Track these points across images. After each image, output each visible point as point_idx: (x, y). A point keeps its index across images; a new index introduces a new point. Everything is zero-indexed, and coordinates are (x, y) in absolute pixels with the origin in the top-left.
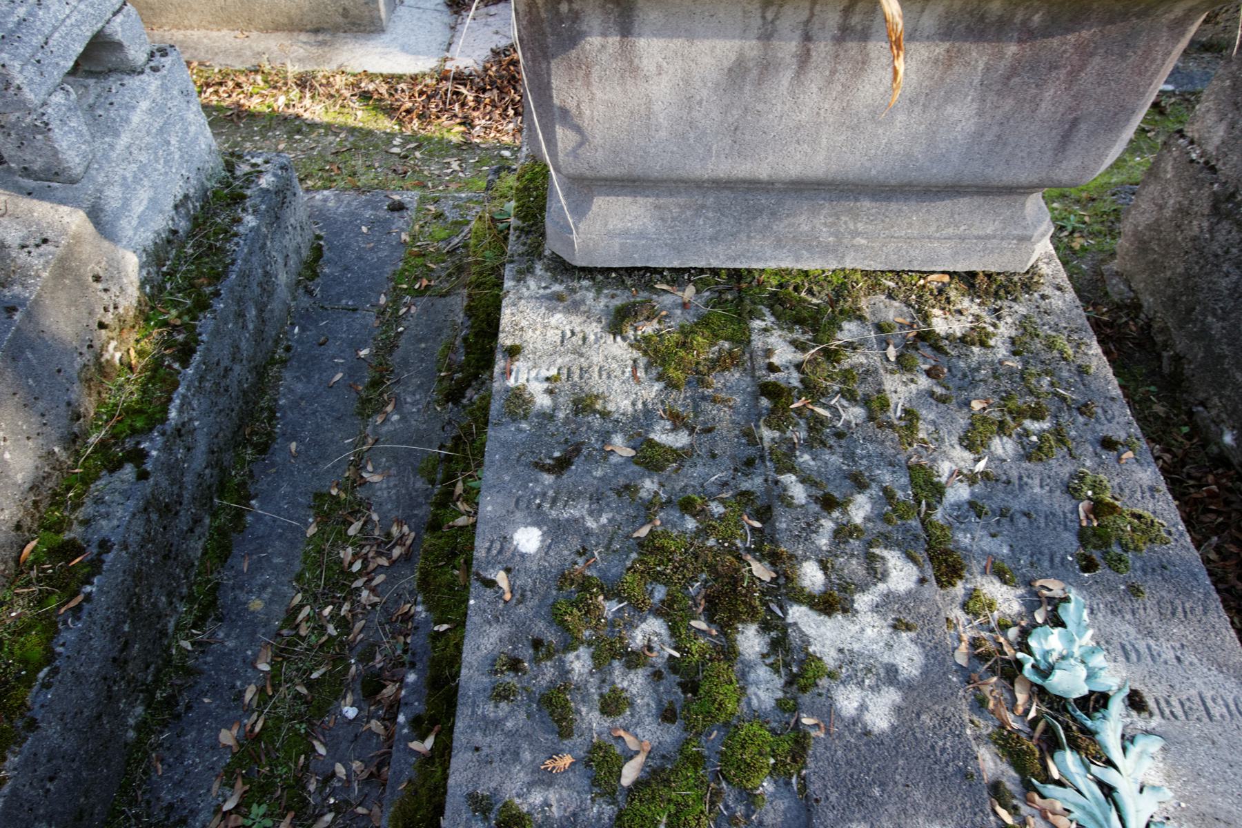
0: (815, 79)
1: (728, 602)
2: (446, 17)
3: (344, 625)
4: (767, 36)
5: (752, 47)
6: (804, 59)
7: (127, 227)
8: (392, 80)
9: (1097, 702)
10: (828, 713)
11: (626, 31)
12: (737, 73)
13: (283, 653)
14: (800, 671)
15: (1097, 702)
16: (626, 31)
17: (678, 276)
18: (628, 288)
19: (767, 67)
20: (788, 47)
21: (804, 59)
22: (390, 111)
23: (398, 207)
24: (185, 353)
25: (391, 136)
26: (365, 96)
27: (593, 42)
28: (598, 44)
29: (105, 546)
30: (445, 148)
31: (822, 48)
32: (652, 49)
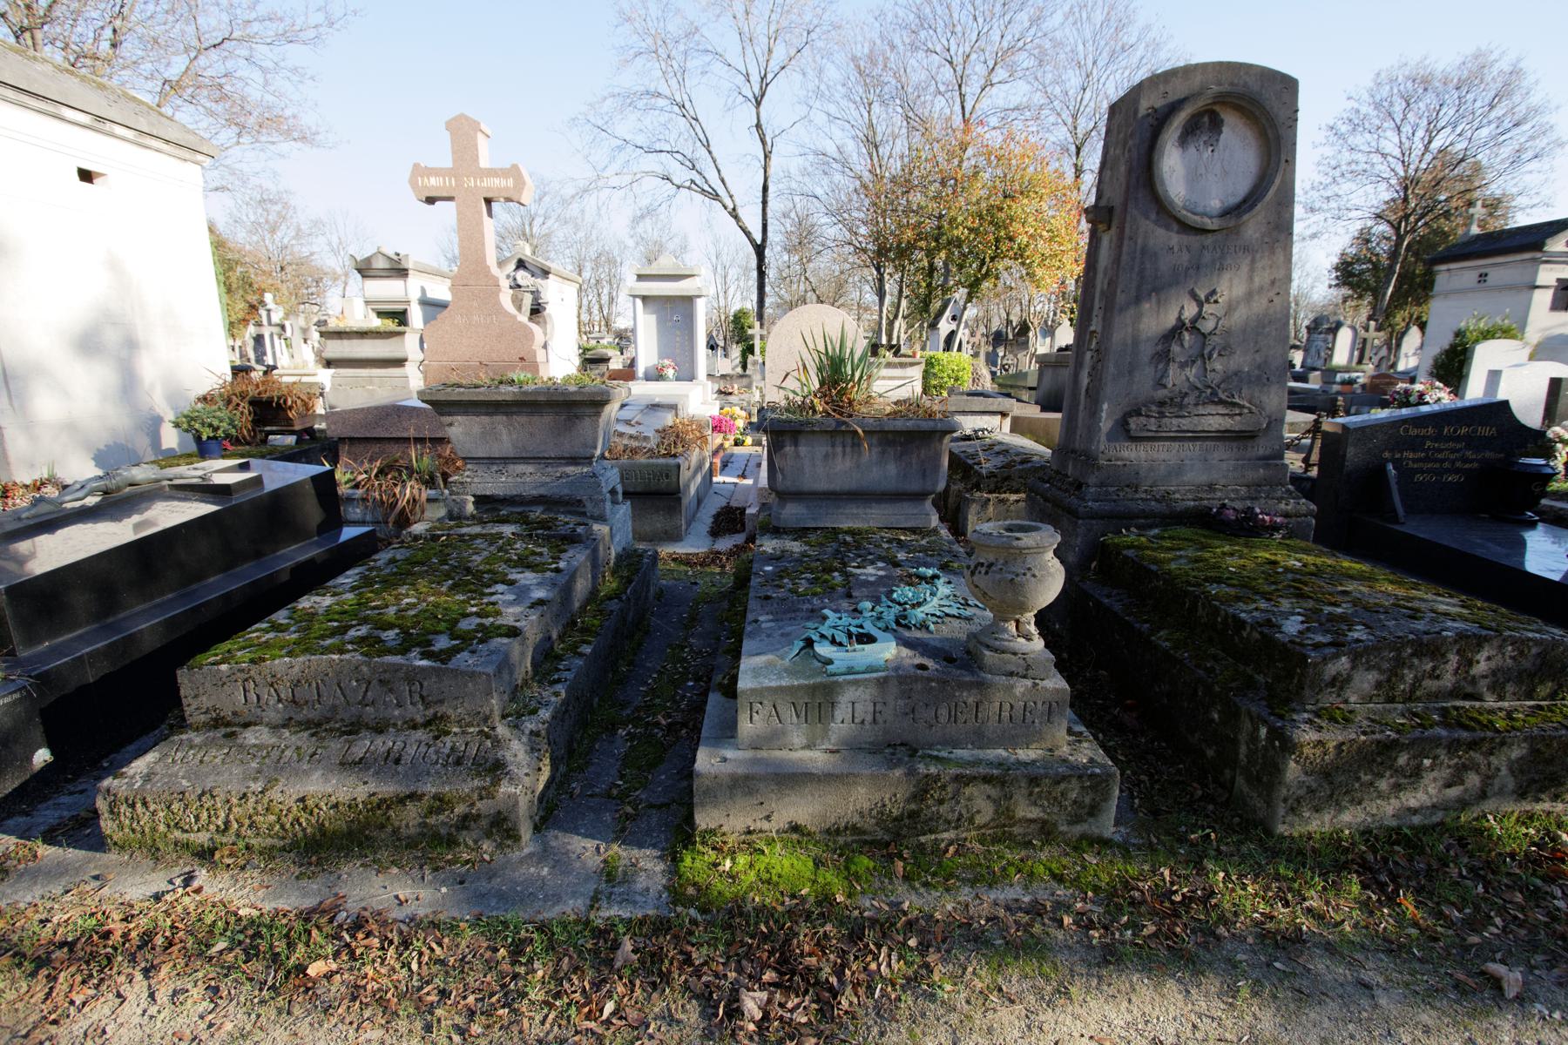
4: (833, 446)
5: (830, 449)
7: (617, 539)
9: (937, 577)
11: (796, 445)
12: (826, 456)
13: (660, 673)
14: (847, 575)
16: (796, 445)
17: (816, 529)
19: (834, 455)
20: (839, 449)
24: (630, 581)
26: (674, 560)
27: (787, 449)
28: (789, 449)
32: (803, 450)
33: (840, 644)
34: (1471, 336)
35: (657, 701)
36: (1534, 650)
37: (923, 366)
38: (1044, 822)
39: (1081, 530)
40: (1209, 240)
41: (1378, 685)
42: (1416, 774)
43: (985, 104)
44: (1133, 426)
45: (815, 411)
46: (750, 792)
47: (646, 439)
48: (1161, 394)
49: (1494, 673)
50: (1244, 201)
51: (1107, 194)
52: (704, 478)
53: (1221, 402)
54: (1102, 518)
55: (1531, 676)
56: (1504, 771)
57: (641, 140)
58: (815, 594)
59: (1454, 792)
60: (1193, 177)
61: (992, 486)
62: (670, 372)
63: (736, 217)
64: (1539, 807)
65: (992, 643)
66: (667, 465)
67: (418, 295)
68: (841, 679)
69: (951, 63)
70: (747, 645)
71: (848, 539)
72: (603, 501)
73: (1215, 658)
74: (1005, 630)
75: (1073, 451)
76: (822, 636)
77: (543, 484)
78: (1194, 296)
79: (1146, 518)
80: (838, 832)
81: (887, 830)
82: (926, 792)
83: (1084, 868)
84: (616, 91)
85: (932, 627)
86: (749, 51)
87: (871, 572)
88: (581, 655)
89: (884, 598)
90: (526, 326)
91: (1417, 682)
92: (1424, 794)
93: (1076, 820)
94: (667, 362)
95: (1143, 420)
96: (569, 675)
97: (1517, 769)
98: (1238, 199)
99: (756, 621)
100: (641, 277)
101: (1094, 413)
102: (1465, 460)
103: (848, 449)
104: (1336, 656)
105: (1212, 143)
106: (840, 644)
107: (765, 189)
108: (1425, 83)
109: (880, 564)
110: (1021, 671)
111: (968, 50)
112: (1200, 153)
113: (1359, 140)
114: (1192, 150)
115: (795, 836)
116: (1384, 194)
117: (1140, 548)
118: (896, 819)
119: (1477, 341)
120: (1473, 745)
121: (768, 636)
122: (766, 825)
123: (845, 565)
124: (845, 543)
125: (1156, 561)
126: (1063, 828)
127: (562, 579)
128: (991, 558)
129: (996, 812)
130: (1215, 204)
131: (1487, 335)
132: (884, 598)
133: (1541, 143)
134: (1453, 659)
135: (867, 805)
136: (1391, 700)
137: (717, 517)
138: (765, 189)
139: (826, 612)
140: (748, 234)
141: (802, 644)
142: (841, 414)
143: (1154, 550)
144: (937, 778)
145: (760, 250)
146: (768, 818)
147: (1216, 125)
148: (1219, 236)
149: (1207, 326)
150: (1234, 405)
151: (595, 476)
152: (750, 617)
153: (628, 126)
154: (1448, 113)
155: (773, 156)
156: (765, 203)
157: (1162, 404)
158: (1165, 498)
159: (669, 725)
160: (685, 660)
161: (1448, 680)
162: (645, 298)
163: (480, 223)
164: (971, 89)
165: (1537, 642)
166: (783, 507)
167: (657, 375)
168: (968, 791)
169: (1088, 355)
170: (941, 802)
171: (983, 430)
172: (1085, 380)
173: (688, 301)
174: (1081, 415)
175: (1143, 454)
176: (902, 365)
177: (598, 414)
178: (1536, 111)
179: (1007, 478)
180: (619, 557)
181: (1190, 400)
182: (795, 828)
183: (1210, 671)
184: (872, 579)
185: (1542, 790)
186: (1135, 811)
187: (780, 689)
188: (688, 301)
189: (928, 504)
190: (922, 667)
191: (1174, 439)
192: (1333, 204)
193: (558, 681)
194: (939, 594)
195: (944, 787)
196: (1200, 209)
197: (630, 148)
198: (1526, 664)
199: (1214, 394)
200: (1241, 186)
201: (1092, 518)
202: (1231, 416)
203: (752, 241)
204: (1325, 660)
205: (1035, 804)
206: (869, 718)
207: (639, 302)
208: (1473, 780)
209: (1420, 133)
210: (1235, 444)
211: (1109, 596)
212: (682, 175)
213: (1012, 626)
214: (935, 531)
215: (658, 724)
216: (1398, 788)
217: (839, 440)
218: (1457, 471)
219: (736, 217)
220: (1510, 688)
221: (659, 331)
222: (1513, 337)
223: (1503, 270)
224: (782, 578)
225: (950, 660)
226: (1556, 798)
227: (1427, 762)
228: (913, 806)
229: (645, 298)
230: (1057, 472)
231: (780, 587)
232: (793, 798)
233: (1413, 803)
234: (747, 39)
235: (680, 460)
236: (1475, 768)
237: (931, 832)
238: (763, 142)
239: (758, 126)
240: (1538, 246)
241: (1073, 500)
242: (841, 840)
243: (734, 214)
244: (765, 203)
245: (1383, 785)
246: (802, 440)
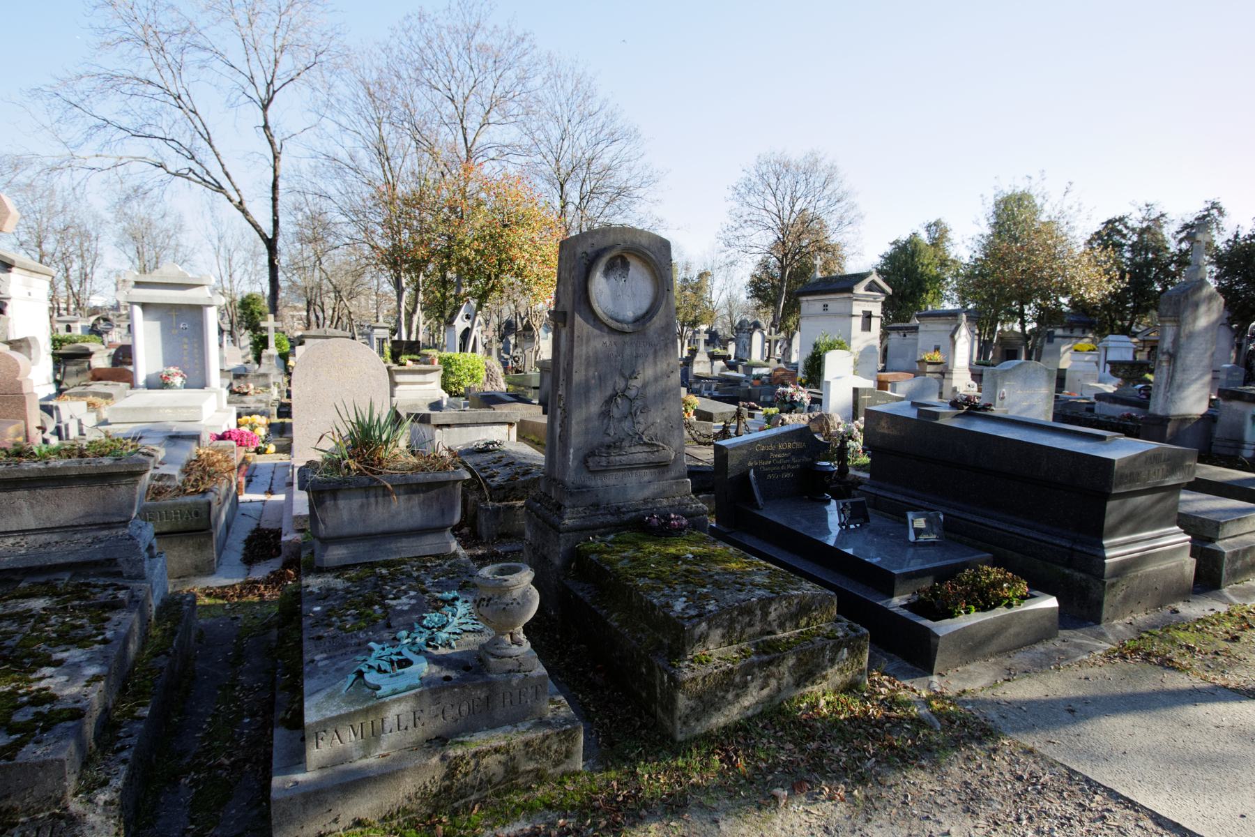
0: (380, 509)
1: (369, 604)
2: (245, 567)
3: (238, 706)
5: (364, 500)
6: (377, 503)
8: (223, 588)
9: (456, 599)
10: (394, 610)
11: (335, 499)
12: (362, 506)
13: (213, 716)
14: (386, 607)
15: (456, 599)
18: (340, 570)
19: (369, 504)
20: (372, 500)
21: (377, 503)
22: (223, 597)
23: (236, 618)
24: (174, 633)
25: (224, 605)
29: (162, 668)
30: (252, 604)
31: (380, 499)
32: (341, 503)
33: (385, 672)
34: (822, 348)
35: (216, 744)
37: (441, 372)
38: (538, 770)
39: (562, 542)
40: (627, 339)
41: (723, 636)
42: (745, 685)
43: (482, 139)
44: (591, 464)
45: (349, 469)
46: (320, 804)
47: (170, 477)
48: (607, 440)
50: (647, 312)
51: (562, 302)
52: (231, 504)
54: (576, 530)
56: (787, 674)
57: (125, 121)
58: (360, 629)
59: (765, 692)
60: (615, 297)
61: (502, 496)
62: (178, 381)
63: (245, 212)
64: (806, 690)
65: (494, 651)
66: (196, 504)
68: (387, 699)
69: (453, 101)
70: (308, 685)
71: (384, 571)
72: (142, 561)
73: (643, 631)
74: (503, 641)
75: (554, 480)
76: (370, 667)
77: (72, 553)
78: (623, 375)
79: (605, 527)
80: (392, 817)
81: (428, 806)
82: (456, 769)
83: (565, 795)
84: (95, 70)
85: (454, 644)
86: (253, 56)
87: (404, 603)
88: (140, 719)
89: (416, 625)
90: (8, 357)
91: (743, 629)
92: (752, 698)
93: (557, 764)
94: (172, 370)
96: (133, 741)
97: (792, 670)
98: (644, 311)
99: (313, 661)
100: (138, 284)
101: (565, 454)
102: (792, 464)
103: (380, 499)
104: (699, 623)
106: (385, 672)
107: (275, 187)
108: (787, 167)
109: (412, 593)
110: (516, 668)
111: (467, 92)
112: (616, 281)
113: (752, 199)
114: (612, 279)
115: (358, 829)
116: (771, 238)
117: (600, 552)
118: (435, 795)
119: (825, 351)
120: (770, 663)
121: (325, 673)
122: (334, 827)
123: (384, 597)
124: (382, 577)
125: (609, 563)
126: (551, 771)
127: (114, 651)
128: (490, 595)
129: (506, 771)
130: (629, 314)
131: (831, 347)
132: (416, 625)
133: (852, 214)
134: (758, 612)
135: (413, 791)
136: (731, 644)
137: (249, 542)
138: (275, 187)
139: (372, 644)
140: (259, 231)
141: (354, 676)
142: (372, 472)
143: (609, 553)
144: (462, 758)
145: (271, 245)
146: (336, 821)
147: (625, 265)
148: (634, 337)
149: (632, 393)
151: (131, 538)
152: (307, 658)
154: (801, 189)
155: (282, 156)
156: (275, 199)
157: (609, 447)
158: (618, 511)
159: (233, 764)
160: (237, 698)
161: (758, 628)
162: (144, 306)
164: (472, 124)
165: (797, 596)
166: (325, 550)
167: (160, 383)
168: (484, 762)
169: (559, 411)
170: (466, 774)
171: (493, 443)
172: (558, 430)
173: (197, 310)
174: (558, 454)
175: (599, 483)
176: (424, 372)
177: (136, 482)
178: (846, 193)
179: (513, 489)
180: (160, 610)
181: (626, 443)
182: (358, 823)
183: (639, 640)
184: (406, 608)
186: (599, 746)
187: (340, 718)
188: (197, 310)
189: (448, 533)
190: (447, 678)
191: (619, 470)
192: (742, 242)
193: (123, 748)
194: (459, 615)
195: (468, 763)
196: (620, 317)
198: (793, 609)
199: (641, 438)
200: (644, 304)
201: (568, 531)
202: (653, 453)
203: (263, 236)
204: (694, 627)
205: (531, 759)
206: (411, 724)
207: (138, 311)
208: (773, 683)
209: (788, 199)
211: (582, 590)
212: (177, 162)
213: (508, 638)
214: (455, 555)
215: (221, 766)
216: (738, 696)
217: (372, 492)
218: (790, 470)
219: (245, 212)
220: (788, 624)
221: (163, 339)
222: (844, 349)
223: (836, 302)
224: (330, 616)
225: (467, 668)
226: (813, 683)
227: (749, 678)
228: (447, 783)
229: (144, 306)
230: (545, 495)
231: (330, 625)
232: (356, 800)
233: (746, 703)
234: (250, 47)
235: (211, 496)
236: (773, 675)
237: (462, 798)
238: (272, 143)
239: (266, 127)
240: (850, 290)
241: (554, 518)
242: (395, 823)
243: (240, 206)
244: (275, 199)
245: (730, 696)
246: (340, 495)
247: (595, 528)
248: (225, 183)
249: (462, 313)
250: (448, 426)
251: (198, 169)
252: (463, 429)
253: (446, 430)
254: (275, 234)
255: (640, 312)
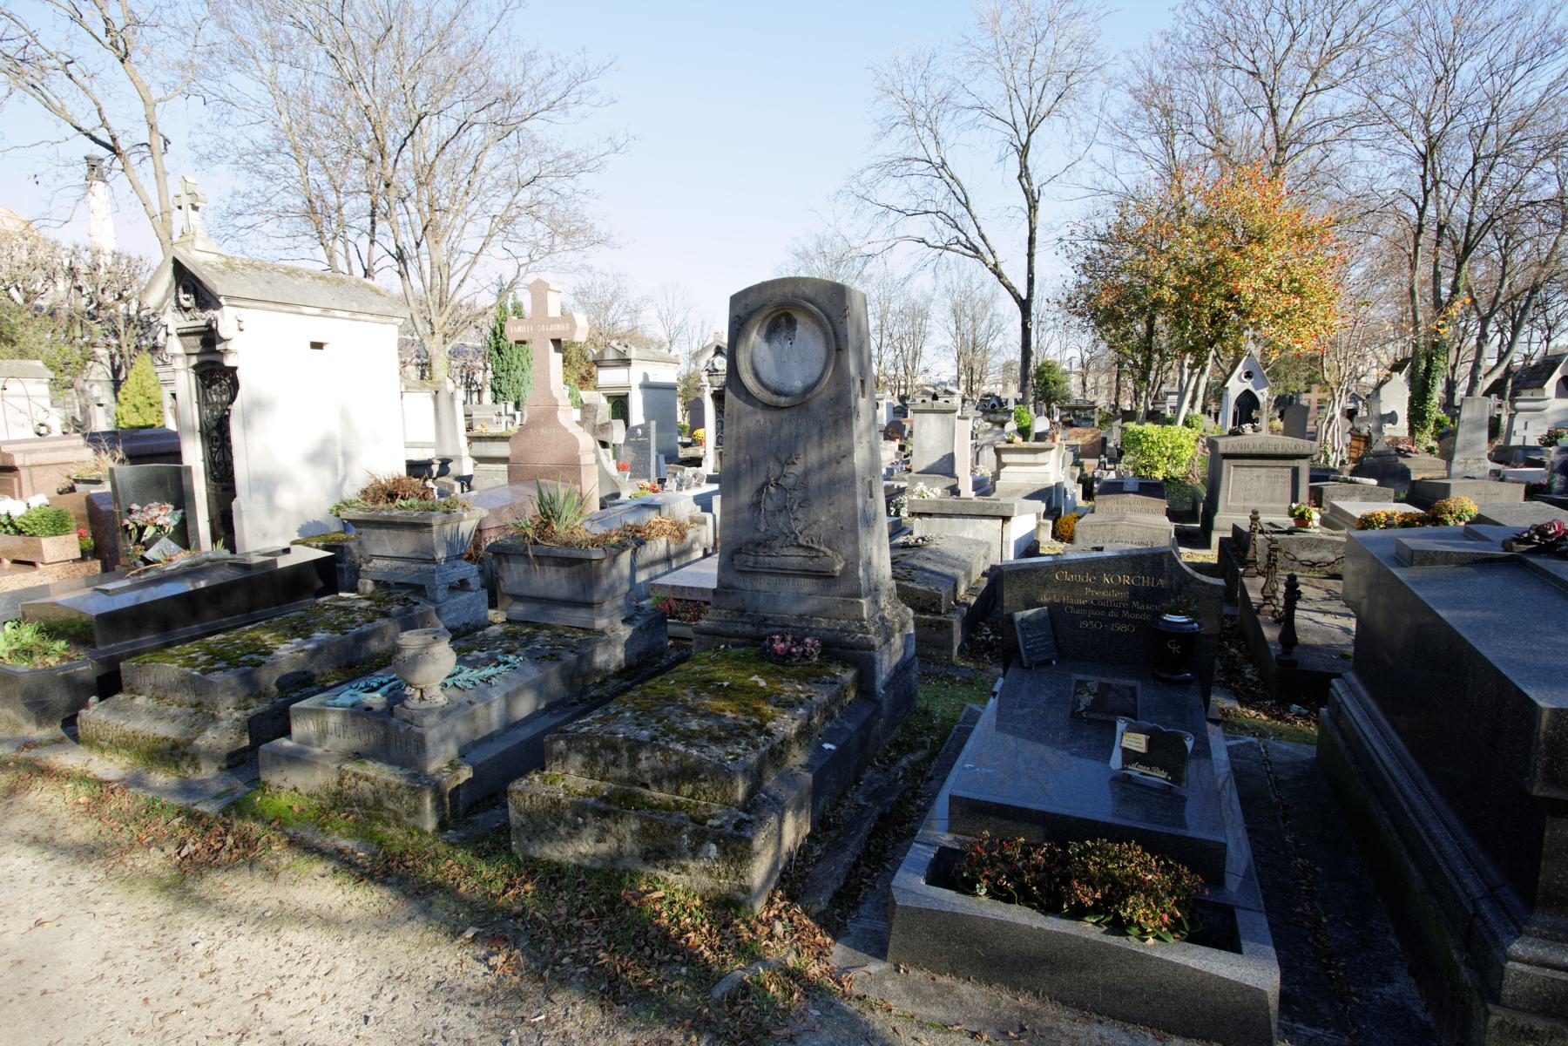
36: (675, 758)
40: (785, 414)
48: (758, 536)
49: (653, 770)
53: (800, 546)
55: (676, 777)
57: (910, 203)
60: (780, 365)
63: (1000, 276)
67: (640, 380)
78: (778, 460)
95: (744, 557)
102: (1133, 611)
105: (791, 339)
107: (1031, 241)
112: (782, 345)
114: (776, 344)
138: (1031, 241)
145: (1025, 306)
147: (791, 323)
150: (812, 549)
153: (893, 192)
155: (1040, 205)
156: (1030, 255)
157: (759, 544)
163: (548, 358)
175: (749, 585)
181: (777, 543)
185: (657, 859)
196: (787, 389)
197: (894, 214)
198: (672, 767)
202: (811, 558)
203: (1017, 297)
210: (820, 582)
218: (1126, 621)
219: (1000, 276)
220: (665, 784)
226: (667, 868)
233: (583, 850)
243: (996, 270)
244: (1030, 255)
247: (729, 636)
248: (983, 248)
249: (1240, 369)
250: (930, 515)
251: (962, 238)
252: (946, 520)
253: (926, 519)
254: (1030, 294)
255: (810, 381)
